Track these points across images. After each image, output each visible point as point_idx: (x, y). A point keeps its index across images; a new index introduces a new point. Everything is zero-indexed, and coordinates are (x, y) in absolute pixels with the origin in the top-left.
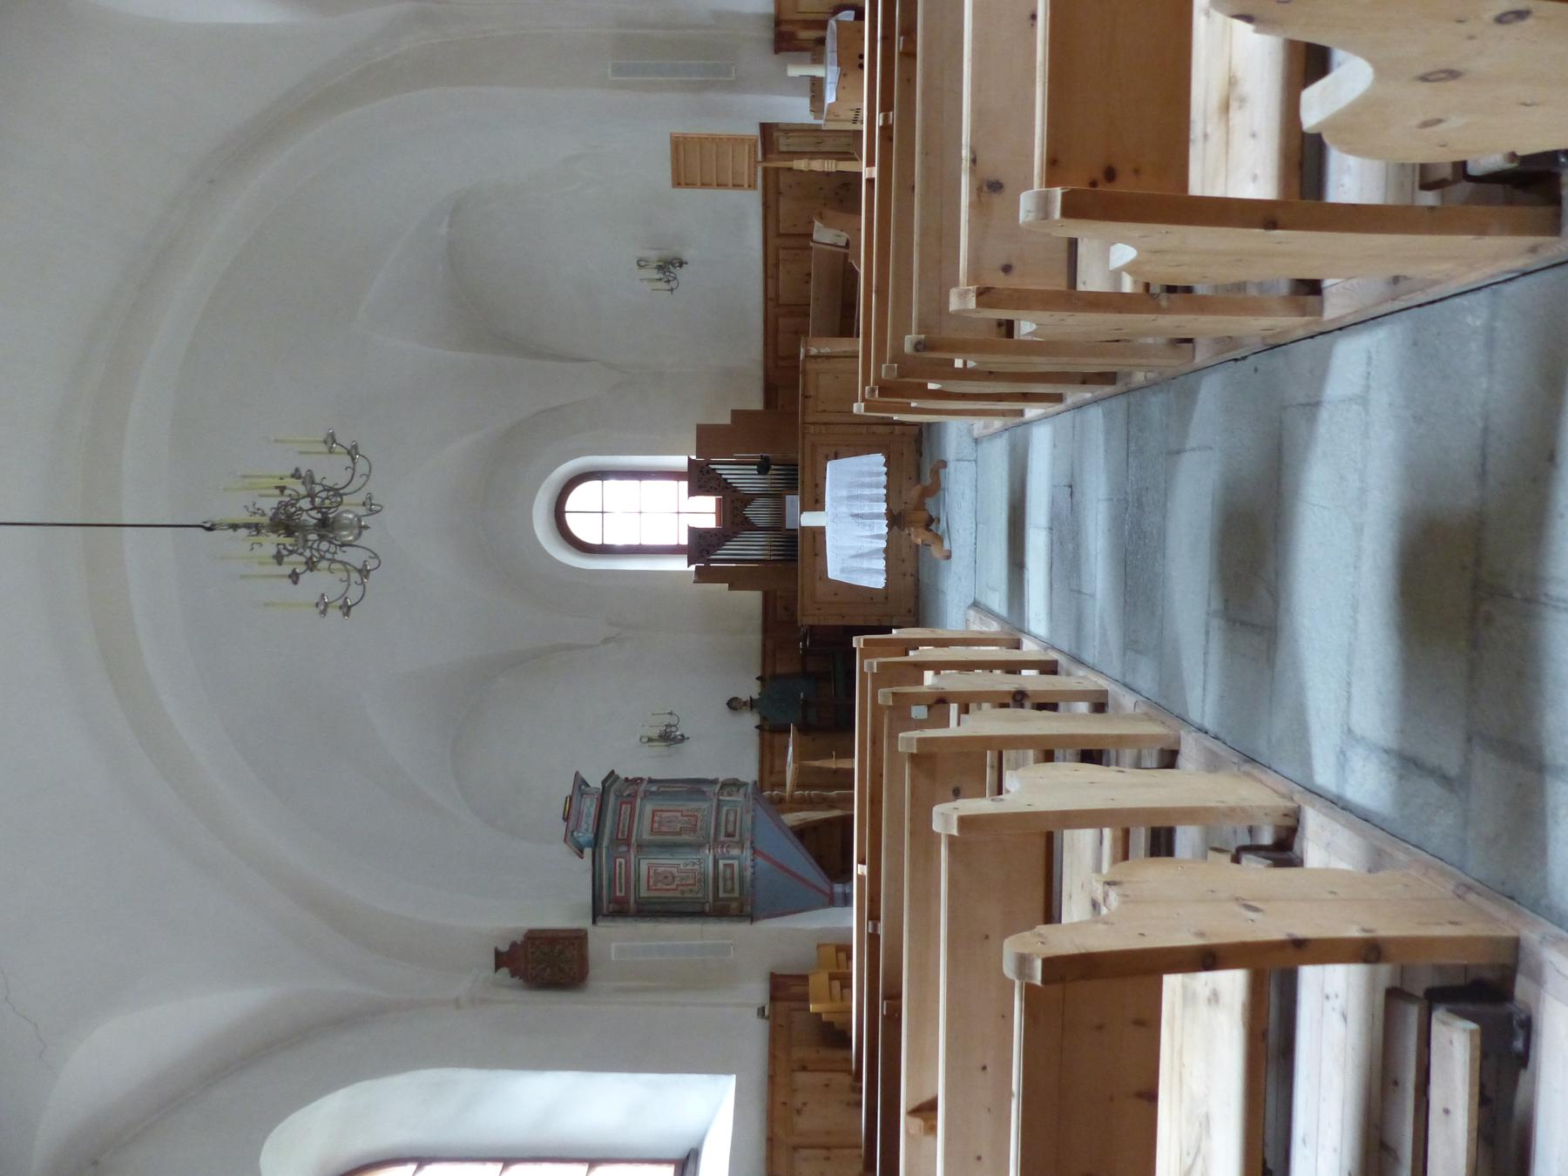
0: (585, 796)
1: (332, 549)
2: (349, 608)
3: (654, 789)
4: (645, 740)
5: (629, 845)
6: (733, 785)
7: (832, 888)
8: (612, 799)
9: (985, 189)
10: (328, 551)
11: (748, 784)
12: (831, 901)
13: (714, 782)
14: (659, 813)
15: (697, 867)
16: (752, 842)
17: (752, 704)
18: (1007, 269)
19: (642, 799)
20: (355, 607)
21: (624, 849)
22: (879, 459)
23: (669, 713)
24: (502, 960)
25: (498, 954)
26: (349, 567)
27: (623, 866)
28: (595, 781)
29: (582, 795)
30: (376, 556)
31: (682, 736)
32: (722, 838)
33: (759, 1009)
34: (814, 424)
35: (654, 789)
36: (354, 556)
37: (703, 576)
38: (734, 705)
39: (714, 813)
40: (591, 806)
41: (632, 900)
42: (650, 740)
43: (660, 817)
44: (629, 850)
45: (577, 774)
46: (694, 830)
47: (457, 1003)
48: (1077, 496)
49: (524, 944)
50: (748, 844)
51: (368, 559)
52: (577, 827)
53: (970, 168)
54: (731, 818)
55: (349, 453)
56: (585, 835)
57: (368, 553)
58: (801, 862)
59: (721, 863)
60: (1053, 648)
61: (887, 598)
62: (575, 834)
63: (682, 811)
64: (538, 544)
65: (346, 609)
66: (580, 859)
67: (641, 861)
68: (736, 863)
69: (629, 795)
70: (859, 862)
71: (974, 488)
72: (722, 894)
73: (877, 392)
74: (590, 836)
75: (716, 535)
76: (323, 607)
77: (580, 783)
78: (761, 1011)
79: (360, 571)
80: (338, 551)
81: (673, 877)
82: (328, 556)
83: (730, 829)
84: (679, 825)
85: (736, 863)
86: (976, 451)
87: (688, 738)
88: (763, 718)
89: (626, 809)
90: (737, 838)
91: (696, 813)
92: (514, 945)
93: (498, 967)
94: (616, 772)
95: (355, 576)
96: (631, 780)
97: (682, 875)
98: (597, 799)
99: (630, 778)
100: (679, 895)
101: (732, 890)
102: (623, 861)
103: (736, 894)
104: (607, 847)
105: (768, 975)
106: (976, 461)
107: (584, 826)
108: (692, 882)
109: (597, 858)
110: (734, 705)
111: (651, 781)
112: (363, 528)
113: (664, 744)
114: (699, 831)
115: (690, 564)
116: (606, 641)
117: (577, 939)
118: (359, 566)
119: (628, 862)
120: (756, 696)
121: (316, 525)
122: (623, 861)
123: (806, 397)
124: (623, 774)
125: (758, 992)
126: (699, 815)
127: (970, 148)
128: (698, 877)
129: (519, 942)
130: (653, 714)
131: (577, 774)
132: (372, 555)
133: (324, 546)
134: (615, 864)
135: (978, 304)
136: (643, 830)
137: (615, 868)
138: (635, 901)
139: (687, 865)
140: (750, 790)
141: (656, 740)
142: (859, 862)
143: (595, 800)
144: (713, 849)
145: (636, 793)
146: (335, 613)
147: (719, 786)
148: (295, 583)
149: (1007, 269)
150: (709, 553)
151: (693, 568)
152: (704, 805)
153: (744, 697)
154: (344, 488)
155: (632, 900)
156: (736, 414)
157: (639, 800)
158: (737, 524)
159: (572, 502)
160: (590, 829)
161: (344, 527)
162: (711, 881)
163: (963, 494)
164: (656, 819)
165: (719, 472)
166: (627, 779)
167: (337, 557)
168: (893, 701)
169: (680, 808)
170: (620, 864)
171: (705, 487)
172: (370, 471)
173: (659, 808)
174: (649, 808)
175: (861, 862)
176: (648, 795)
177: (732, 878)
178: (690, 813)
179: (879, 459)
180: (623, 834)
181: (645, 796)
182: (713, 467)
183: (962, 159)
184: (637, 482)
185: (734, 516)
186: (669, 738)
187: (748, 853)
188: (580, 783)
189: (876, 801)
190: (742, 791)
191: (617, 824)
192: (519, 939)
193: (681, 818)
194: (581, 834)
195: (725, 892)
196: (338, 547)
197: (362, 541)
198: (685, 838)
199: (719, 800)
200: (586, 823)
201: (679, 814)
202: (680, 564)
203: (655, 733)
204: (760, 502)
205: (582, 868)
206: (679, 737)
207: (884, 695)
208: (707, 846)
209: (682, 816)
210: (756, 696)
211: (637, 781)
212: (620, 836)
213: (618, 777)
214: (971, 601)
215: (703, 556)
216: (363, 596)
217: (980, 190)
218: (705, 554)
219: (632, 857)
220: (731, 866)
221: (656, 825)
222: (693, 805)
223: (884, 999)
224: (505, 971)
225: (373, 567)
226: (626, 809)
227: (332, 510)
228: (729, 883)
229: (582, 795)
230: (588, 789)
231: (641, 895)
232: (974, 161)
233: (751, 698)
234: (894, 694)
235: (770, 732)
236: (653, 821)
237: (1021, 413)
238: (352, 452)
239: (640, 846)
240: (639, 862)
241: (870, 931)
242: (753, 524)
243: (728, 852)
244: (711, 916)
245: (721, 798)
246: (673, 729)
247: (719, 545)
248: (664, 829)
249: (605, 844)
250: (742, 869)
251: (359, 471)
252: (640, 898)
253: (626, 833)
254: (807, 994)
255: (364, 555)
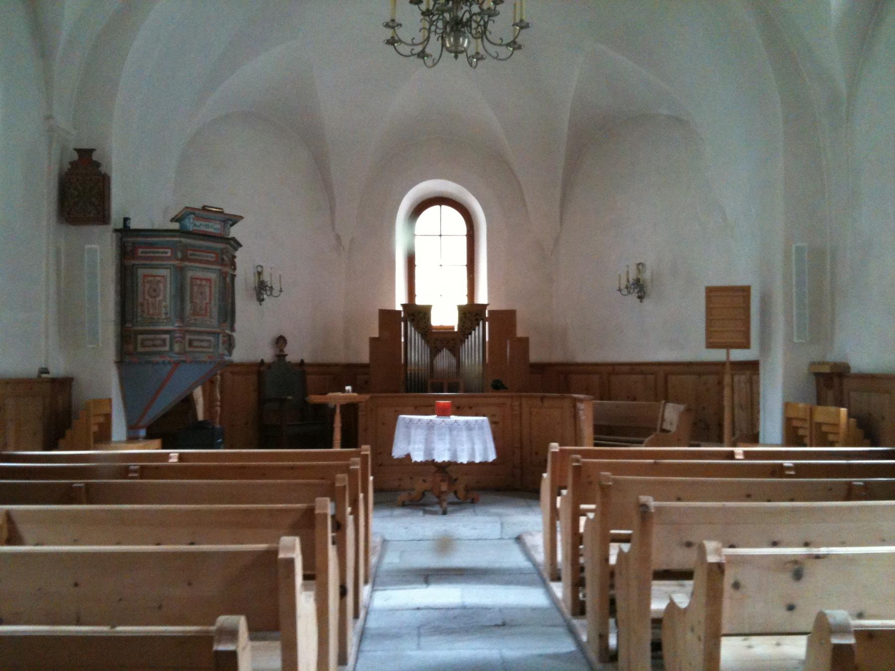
0: (223, 224)
1: (439, 31)
2: (393, 44)
3: (228, 280)
4: (259, 269)
5: (182, 260)
6: (230, 344)
7: (142, 427)
8: (220, 246)
9: (796, 567)
10: (437, 27)
11: (231, 356)
12: (132, 428)
13: (232, 329)
14: (208, 284)
15: (164, 316)
16: (184, 362)
17: (281, 356)
18: (736, 586)
19: (220, 270)
20: (394, 49)
21: (179, 255)
22: (492, 457)
23: (281, 289)
24: (85, 154)
25: (90, 151)
26: (426, 43)
27: (164, 255)
28: (235, 232)
29: (224, 221)
30: (434, 65)
31: (263, 300)
32: (188, 337)
33: (46, 369)
34: (520, 405)
35: (228, 280)
36: (434, 47)
37: (388, 317)
38: (281, 341)
39: (208, 330)
40: (215, 229)
41: (136, 262)
42: (260, 274)
43: (205, 285)
44: (177, 259)
45: (242, 218)
46: (195, 313)
47: (49, 118)
48: (500, 630)
49: (99, 173)
50: (183, 358)
51: (432, 58)
52: (198, 217)
53: (812, 555)
54: (205, 344)
55: (514, 42)
56: (191, 224)
57: (438, 58)
58: (166, 400)
59: (167, 336)
60: (367, 613)
61: (381, 465)
62: (192, 216)
63: (210, 303)
64: (415, 183)
65: (392, 42)
66: (170, 218)
67: (169, 270)
68: (167, 348)
69: (223, 260)
70: (181, 455)
71: (479, 537)
72: (140, 337)
73: (576, 464)
74: (191, 228)
75: (426, 326)
76: (392, 25)
77: (234, 220)
78: (45, 371)
79: (423, 51)
80: (437, 36)
81: (155, 297)
82: (433, 28)
83: (195, 344)
84: (198, 301)
85: (167, 348)
86: (510, 539)
87: (261, 304)
88: (270, 366)
89: (212, 257)
90: (188, 349)
91: (208, 314)
92: (98, 165)
93: (79, 151)
94: (240, 249)
95: (418, 49)
96: (233, 260)
97: (157, 303)
98: (221, 234)
99: (236, 260)
100: (140, 300)
101: (143, 346)
102: (169, 254)
103: (140, 349)
104: (180, 242)
105: (70, 376)
106: (501, 539)
107: (198, 223)
108: (151, 311)
109: (170, 234)
110: (281, 341)
111: (233, 277)
112: (457, 54)
113: (257, 285)
114: (193, 318)
115: (403, 306)
116: (338, 238)
117: (103, 218)
118: (428, 51)
119: (169, 258)
120: (288, 359)
121: (457, 17)
122: (169, 254)
123: (542, 399)
124: (238, 254)
125: (58, 368)
126: (206, 318)
127: (827, 554)
128: (155, 317)
129: (100, 169)
130: (280, 276)
131: (242, 218)
132: (435, 61)
133: (440, 24)
134: (167, 248)
135: (711, 564)
136: (194, 272)
137: (164, 248)
138: (134, 265)
139: (166, 307)
140: (227, 358)
141: (259, 278)
142: (181, 455)
143: (219, 232)
144: (179, 330)
145: (225, 265)
146: (389, 33)
147: (228, 332)
148: (527, 26)
149: (736, 586)
150: (412, 321)
151: (399, 308)
152: (215, 322)
153: (287, 350)
154: (489, 41)
155: (136, 262)
156: (525, 341)
157: (219, 267)
158: (435, 343)
159: (448, 211)
160: (195, 228)
161: (456, 39)
162: (152, 328)
163: (475, 529)
164: (204, 283)
165: (477, 328)
166: (234, 257)
167: (432, 35)
168: (340, 487)
169: (213, 302)
170: (167, 253)
171: (465, 317)
172: (500, 59)
173: (213, 285)
174: (213, 276)
175: (181, 457)
176: (223, 276)
177: (154, 346)
178: (208, 310)
179: (492, 457)
180: (191, 255)
181: (223, 273)
182: (481, 323)
183: (819, 547)
184: (465, 263)
185: (441, 341)
186: (261, 289)
187: (176, 358)
188: (234, 220)
189: (241, 472)
190: (226, 352)
191: (200, 249)
192: (103, 169)
193: (204, 303)
194: (192, 221)
195: (143, 340)
196: (441, 35)
197: (445, 53)
198: (188, 306)
199: (219, 334)
200: (201, 224)
201: (207, 301)
202: (400, 300)
203: (266, 277)
204: (454, 361)
205: (162, 222)
206: (262, 297)
207: (344, 479)
208: (181, 325)
209: (207, 304)
210: (288, 359)
211: (233, 265)
212: (189, 252)
213: (236, 250)
214: (387, 537)
215: (409, 316)
216: (401, 55)
217: (796, 562)
218: (412, 318)
219: (172, 263)
220: (164, 345)
221: (198, 282)
222: (215, 311)
223: (87, 484)
224: (75, 156)
225: (426, 61)
226: (212, 257)
227: (469, 29)
228: (151, 343)
229: (224, 221)
230: (229, 226)
231: (139, 270)
232: (818, 557)
233: (287, 355)
234: (344, 487)
235: (259, 369)
236: (201, 279)
237: (557, 578)
238: (514, 44)
239: (181, 270)
240: (167, 268)
241: (132, 467)
242: (435, 355)
243: (177, 342)
244: (122, 328)
245: (221, 335)
246: (269, 293)
247: (417, 328)
248: (195, 289)
249: (183, 240)
250: (160, 353)
251: (499, 49)
252: (137, 268)
253: (192, 257)
254: (653, 628)
255: (436, 56)
